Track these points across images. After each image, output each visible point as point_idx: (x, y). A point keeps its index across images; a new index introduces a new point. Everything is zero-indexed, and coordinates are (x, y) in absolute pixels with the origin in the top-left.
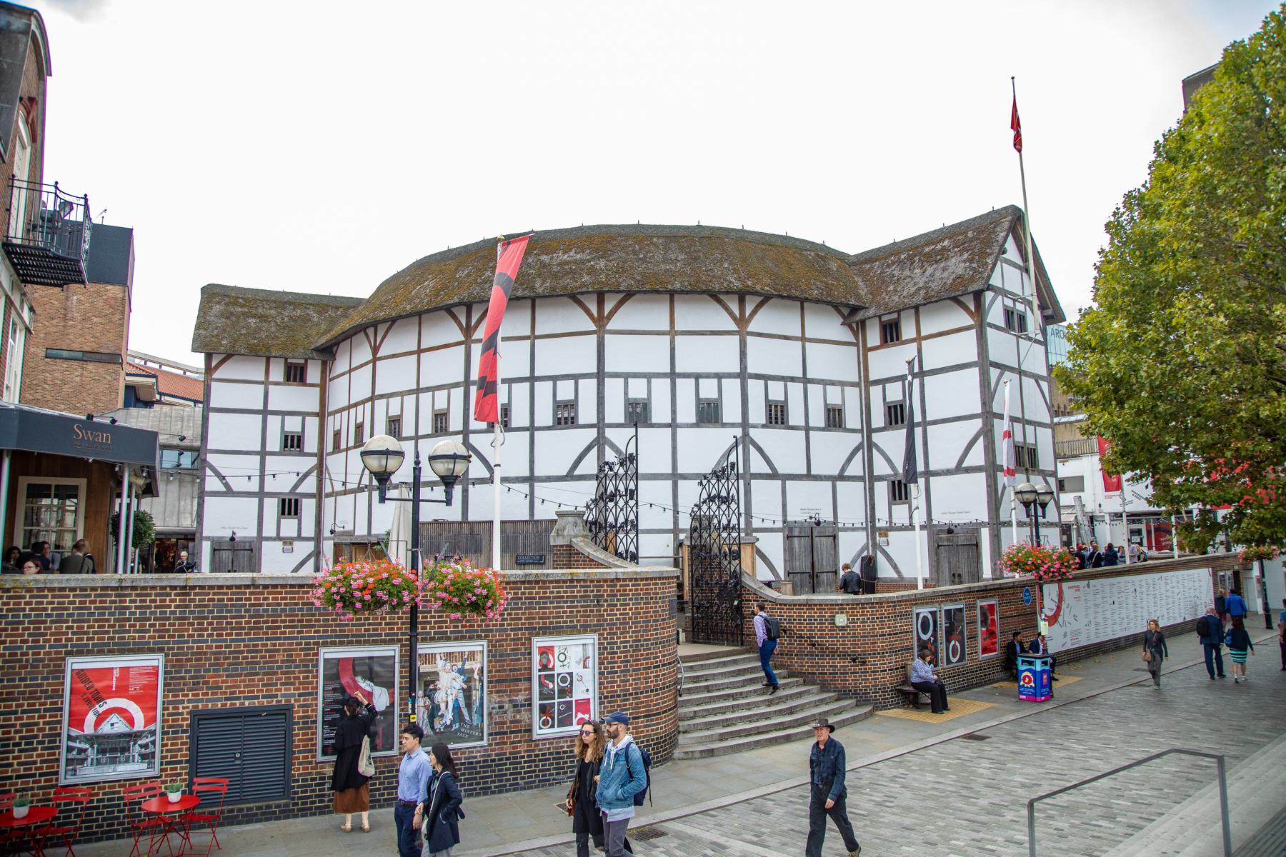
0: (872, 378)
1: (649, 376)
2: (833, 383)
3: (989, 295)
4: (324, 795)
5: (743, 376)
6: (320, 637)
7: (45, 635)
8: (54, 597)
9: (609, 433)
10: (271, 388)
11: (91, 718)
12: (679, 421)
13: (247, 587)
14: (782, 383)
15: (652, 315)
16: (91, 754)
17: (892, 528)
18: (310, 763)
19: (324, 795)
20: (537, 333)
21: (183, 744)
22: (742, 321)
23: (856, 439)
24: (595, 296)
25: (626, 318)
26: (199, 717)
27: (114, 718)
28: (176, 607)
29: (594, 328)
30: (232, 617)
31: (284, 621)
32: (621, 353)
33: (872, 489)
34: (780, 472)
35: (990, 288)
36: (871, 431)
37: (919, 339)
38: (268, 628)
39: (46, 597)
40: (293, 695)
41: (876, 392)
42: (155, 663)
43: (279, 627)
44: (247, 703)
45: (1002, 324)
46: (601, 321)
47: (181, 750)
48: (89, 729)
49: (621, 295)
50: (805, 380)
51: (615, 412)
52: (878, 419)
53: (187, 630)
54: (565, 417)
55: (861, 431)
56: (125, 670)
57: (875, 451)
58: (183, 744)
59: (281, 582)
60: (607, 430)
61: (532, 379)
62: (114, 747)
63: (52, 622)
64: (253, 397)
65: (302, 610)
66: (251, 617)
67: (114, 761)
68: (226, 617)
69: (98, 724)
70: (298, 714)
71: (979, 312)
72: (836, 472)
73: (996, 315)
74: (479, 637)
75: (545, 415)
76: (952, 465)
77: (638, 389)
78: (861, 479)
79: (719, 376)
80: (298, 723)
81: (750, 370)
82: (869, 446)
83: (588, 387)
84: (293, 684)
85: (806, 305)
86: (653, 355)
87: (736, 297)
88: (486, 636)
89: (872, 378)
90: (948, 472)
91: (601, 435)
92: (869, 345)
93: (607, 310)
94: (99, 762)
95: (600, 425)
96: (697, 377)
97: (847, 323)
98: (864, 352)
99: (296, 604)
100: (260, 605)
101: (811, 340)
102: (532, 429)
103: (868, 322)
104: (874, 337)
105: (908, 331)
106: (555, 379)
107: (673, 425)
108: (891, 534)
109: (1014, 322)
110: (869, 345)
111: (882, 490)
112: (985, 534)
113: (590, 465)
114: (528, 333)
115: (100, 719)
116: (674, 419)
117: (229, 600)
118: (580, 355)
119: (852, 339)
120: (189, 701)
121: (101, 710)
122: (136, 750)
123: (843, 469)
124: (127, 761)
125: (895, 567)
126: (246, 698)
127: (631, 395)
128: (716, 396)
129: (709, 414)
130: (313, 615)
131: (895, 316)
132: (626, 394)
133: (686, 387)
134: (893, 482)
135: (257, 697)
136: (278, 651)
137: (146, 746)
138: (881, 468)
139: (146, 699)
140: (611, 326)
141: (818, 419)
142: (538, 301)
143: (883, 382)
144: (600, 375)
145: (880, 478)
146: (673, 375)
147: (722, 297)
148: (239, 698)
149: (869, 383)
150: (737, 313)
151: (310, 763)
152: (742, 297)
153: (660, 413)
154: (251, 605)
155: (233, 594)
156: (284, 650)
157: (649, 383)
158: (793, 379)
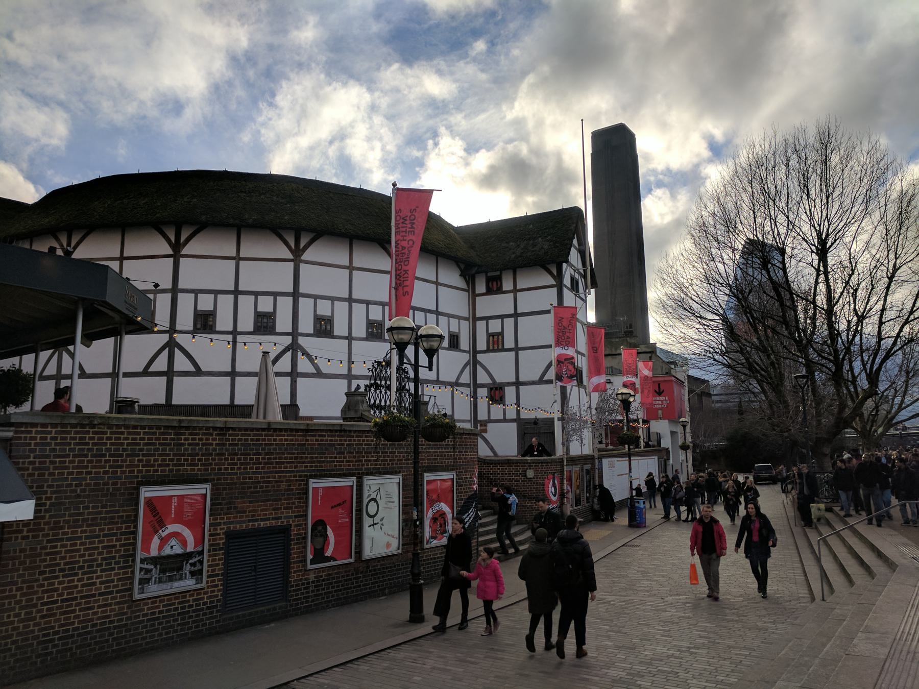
0: (478, 315)
1: (333, 299)
2: (453, 316)
3: (565, 265)
4: (308, 597)
6: (308, 471)
7: (121, 467)
8: (129, 433)
9: (302, 341)
11: (156, 542)
12: (354, 335)
13: (263, 430)
15: (337, 254)
16: (155, 574)
17: (490, 421)
18: (301, 571)
19: (308, 597)
21: (220, 559)
23: (465, 357)
26: (230, 535)
27: (173, 542)
28: (217, 445)
29: (291, 257)
30: (254, 454)
31: (286, 458)
33: (475, 392)
35: (567, 261)
36: (475, 352)
37: (515, 291)
38: (277, 463)
39: (123, 433)
40: (291, 517)
41: (481, 325)
42: (203, 492)
43: (283, 463)
44: (262, 523)
45: (569, 285)
46: (297, 253)
47: (218, 565)
48: (154, 552)
50: (437, 313)
51: (306, 324)
52: (482, 344)
53: (224, 464)
54: (265, 324)
55: (469, 352)
56: (181, 497)
57: (478, 366)
58: (220, 559)
59: (286, 427)
60: (300, 338)
61: (236, 292)
62: (170, 566)
63: (128, 455)
65: (296, 449)
66: (266, 454)
67: (171, 579)
68: (249, 454)
69: (161, 547)
70: (294, 531)
71: (559, 277)
72: (453, 380)
73: (567, 281)
74: (396, 473)
75: (247, 322)
76: (537, 378)
77: (324, 309)
78: (468, 385)
80: (293, 540)
82: (474, 363)
83: (285, 304)
84: (291, 508)
85: (439, 258)
88: (400, 472)
89: (478, 315)
90: (533, 383)
91: (295, 340)
92: (477, 292)
94: (160, 581)
95: (295, 333)
96: (368, 303)
98: (474, 296)
99: (294, 445)
100: (272, 444)
102: (235, 333)
103: (477, 275)
104: (481, 287)
105: (507, 285)
106: (256, 294)
107: (350, 338)
108: (490, 426)
109: (574, 287)
110: (477, 292)
111: (483, 392)
112: (558, 426)
114: (233, 253)
115: (164, 541)
117: (252, 440)
118: (278, 277)
119: (465, 287)
120: (225, 524)
121: (164, 534)
122: (187, 568)
124: (181, 579)
125: (492, 449)
126: (262, 520)
127: (318, 313)
130: (304, 453)
131: (498, 273)
132: (315, 311)
133: (359, 309)
134: (491, 389)
135: (268, 519)
136: (282, 481)
137: (193, 565)
138: (483, 378)
139: (195, 524)
143: (487, 319)
144: (296, 295)
145: (482, 386)
146: (350, 300)
148: (257, 520)
151: (301, 571)
154: (266, 444)
155: (254, 435)
156: (287, 481)
157: (333, 304)
158: (430, 311)
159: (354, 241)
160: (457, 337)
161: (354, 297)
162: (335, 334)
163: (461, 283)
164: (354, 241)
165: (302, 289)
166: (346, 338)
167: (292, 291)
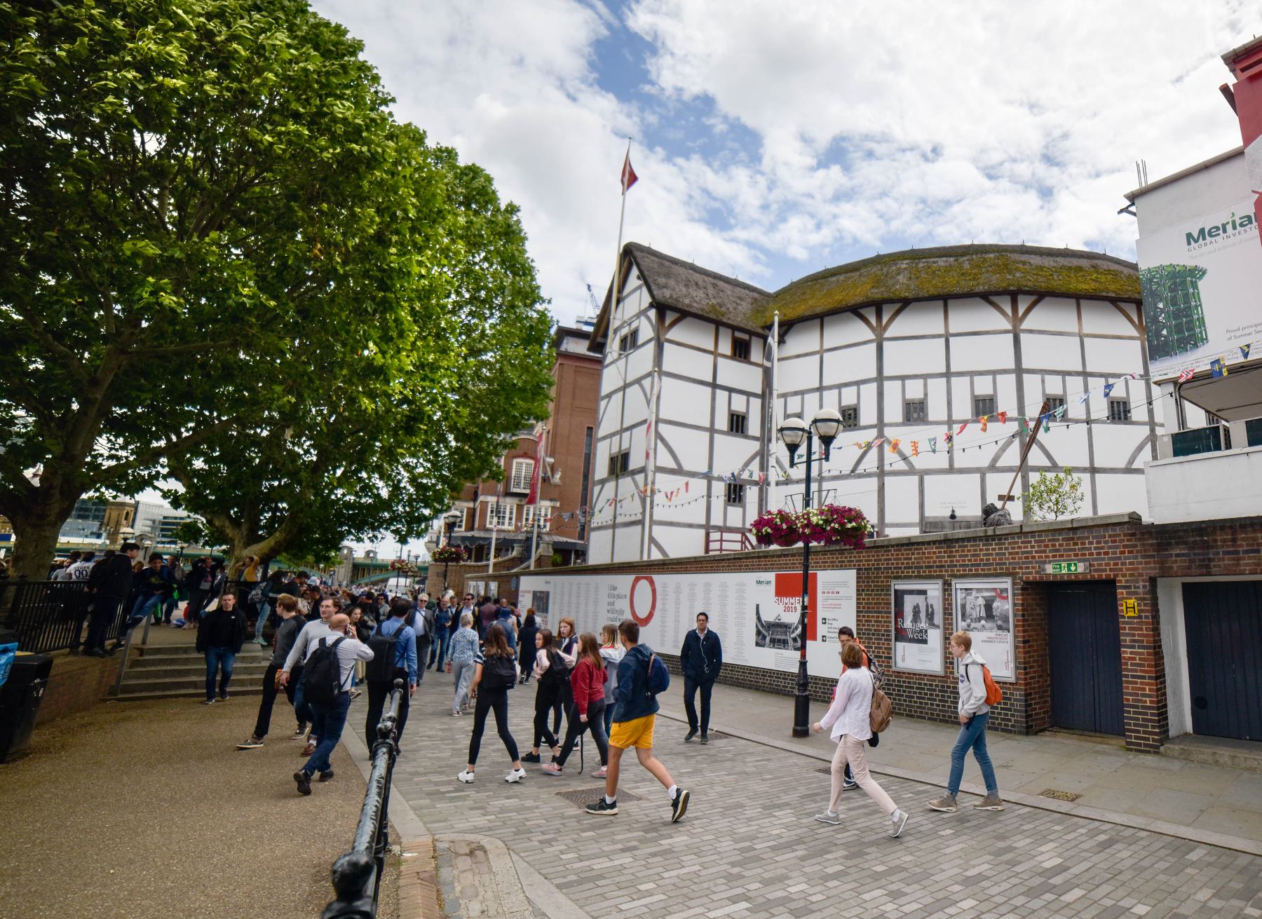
1: (925, 377)
5: (1019, 371)
9: (888, 432)
14: (1060, 378)
20: (826, 346)
22: (1017, 320)
23: (1146, 430)
24: (873, 309)
25: (903, 325)
29: (873, 337)
32: (899, 358)
34: (1060, 464)
46: (880, 330)
49: (897, 306)
50: (1085, 374)
51: (894, 412)
61: (821, 389)
77: (914, 391)
79: (994, 373)
81: (1024, 366)
83: (870, 391)
86: (928, 356)
87: (1009, 298)
93: (885, 320)
95: (880, 425)
96: (972, 374)
101: (1088, 336)
107: (950, 422)
113: (870, 463)
114: (818, 348)
123: (1131, 461)
128: (991, 392)
129: (985, 408)
140: (887, 335)
141: (1100, 409)
142: (826, 319)
146: (948, 374)
147: (993, 298)
150: (1010, 313)
152: (1014, 296)
158: (1069, 373)
159: (950, 302)
160: (1125, 403)
164: (950, 302)
165: (886, 373)
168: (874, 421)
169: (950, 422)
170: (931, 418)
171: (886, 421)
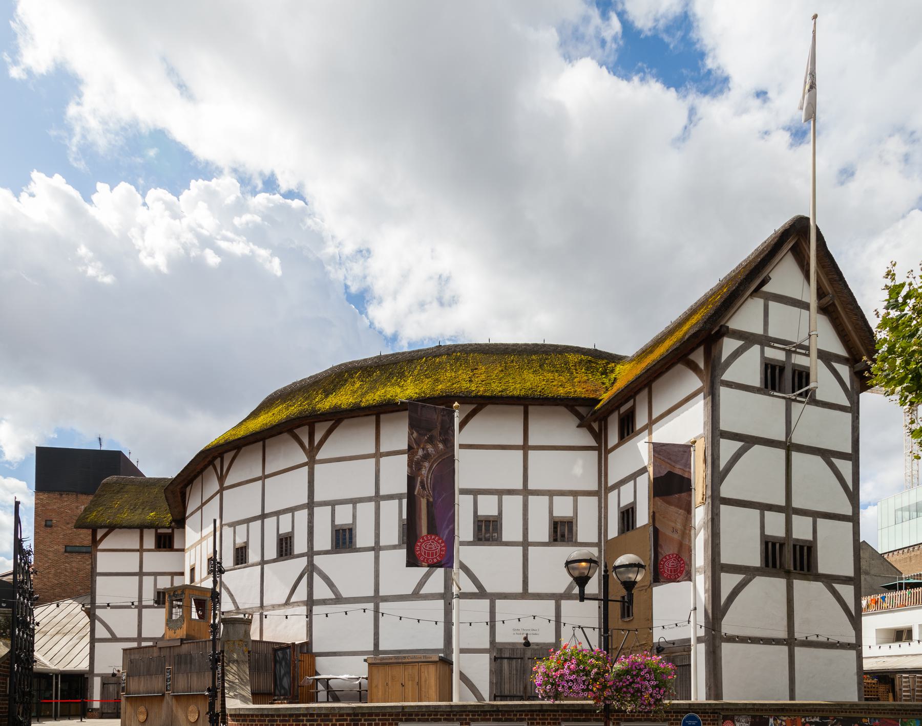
1: (354, 502)
10: (145, 554)
12: (382, 543)
51: (323, 540)
61: (263, 516)
64: (130, 562)
77: (344, 516)
97: (584, 423)
106: (277, 514)
110: (610, 446)
116: (377, 541)
127: (336, 523)
132: (333, 521)
149: (609, 489)
153: (364, 537)
157: (354, 508)
161: (383, 492)
162: (358, 546)
163: (585, 438)
165: (317, 498)
166: (372, 549)
167: (306, 501)
168: (305, 549)
169: (377, 548)
170: (359, 544)
171: (315, 549)
